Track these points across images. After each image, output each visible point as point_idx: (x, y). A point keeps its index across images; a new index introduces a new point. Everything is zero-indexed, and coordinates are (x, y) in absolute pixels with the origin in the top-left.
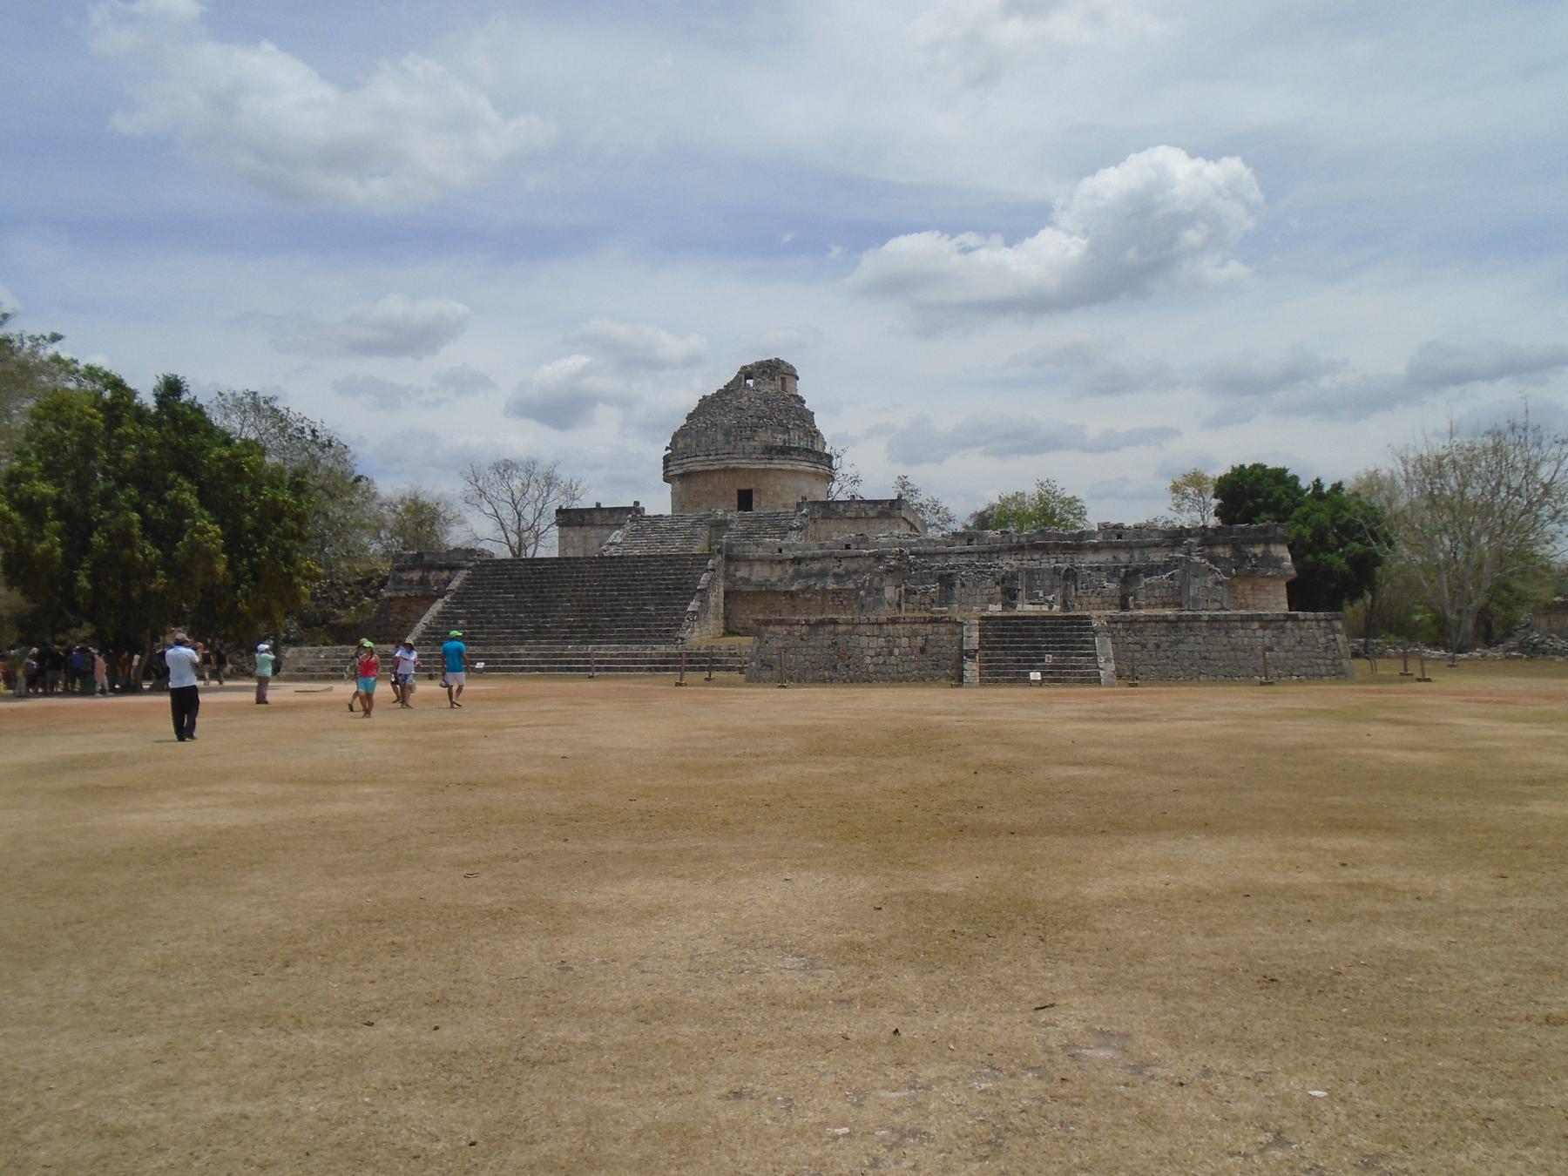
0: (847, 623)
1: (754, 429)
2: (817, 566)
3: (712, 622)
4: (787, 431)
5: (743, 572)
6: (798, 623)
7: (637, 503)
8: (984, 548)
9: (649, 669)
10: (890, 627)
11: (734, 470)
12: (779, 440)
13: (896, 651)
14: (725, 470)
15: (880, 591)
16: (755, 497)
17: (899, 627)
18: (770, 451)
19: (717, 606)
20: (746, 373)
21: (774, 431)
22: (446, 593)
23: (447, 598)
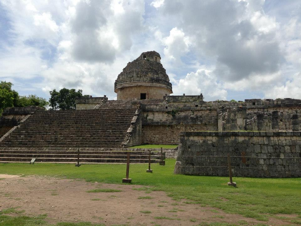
0: (243, 135)
1: (147, 73)
2: (183, 114)
3: (137, 138)
4: (157, 74)
5: (150, 117)
6: (210, 135)
7: (105, 96)
8: (262, 106)
9: (108, 161)
10: (276, 139)
11: (140, 86)
12: (155, 76)
13: (282, 156)
14: (136, 86)
15: (234, 120)
16: (147, 96)
17: (282, 138)
18: (152, 80)
19: (139, 130)
20: (144, 55)
21: (153, 74)
22: (19, 124)
23: (19, 126)
